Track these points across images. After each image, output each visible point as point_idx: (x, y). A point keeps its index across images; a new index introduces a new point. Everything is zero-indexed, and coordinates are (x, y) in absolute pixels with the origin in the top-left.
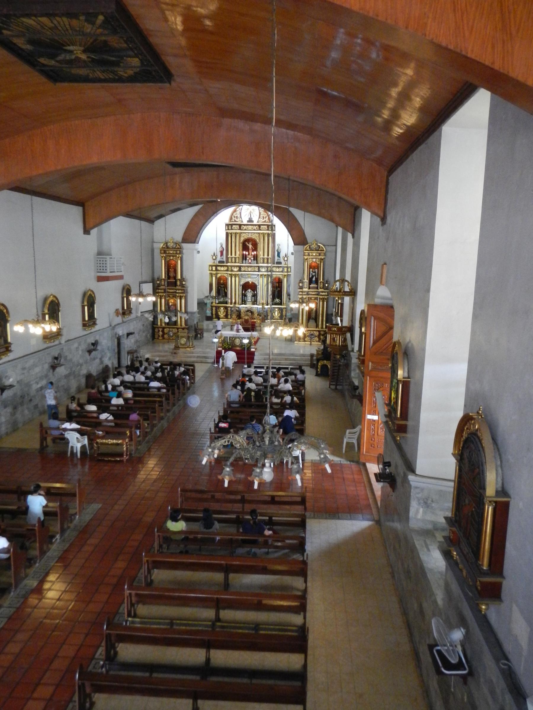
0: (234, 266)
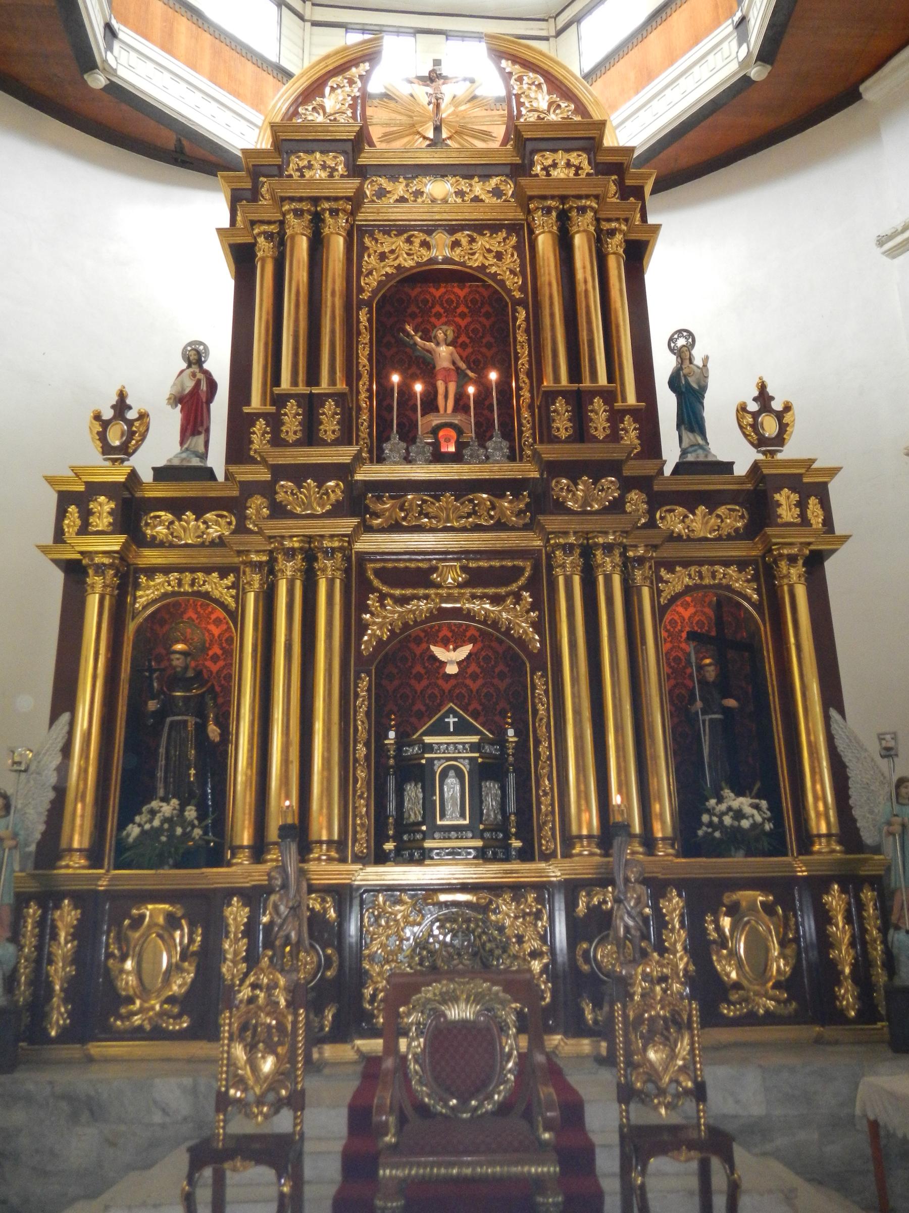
0: (298, 474)
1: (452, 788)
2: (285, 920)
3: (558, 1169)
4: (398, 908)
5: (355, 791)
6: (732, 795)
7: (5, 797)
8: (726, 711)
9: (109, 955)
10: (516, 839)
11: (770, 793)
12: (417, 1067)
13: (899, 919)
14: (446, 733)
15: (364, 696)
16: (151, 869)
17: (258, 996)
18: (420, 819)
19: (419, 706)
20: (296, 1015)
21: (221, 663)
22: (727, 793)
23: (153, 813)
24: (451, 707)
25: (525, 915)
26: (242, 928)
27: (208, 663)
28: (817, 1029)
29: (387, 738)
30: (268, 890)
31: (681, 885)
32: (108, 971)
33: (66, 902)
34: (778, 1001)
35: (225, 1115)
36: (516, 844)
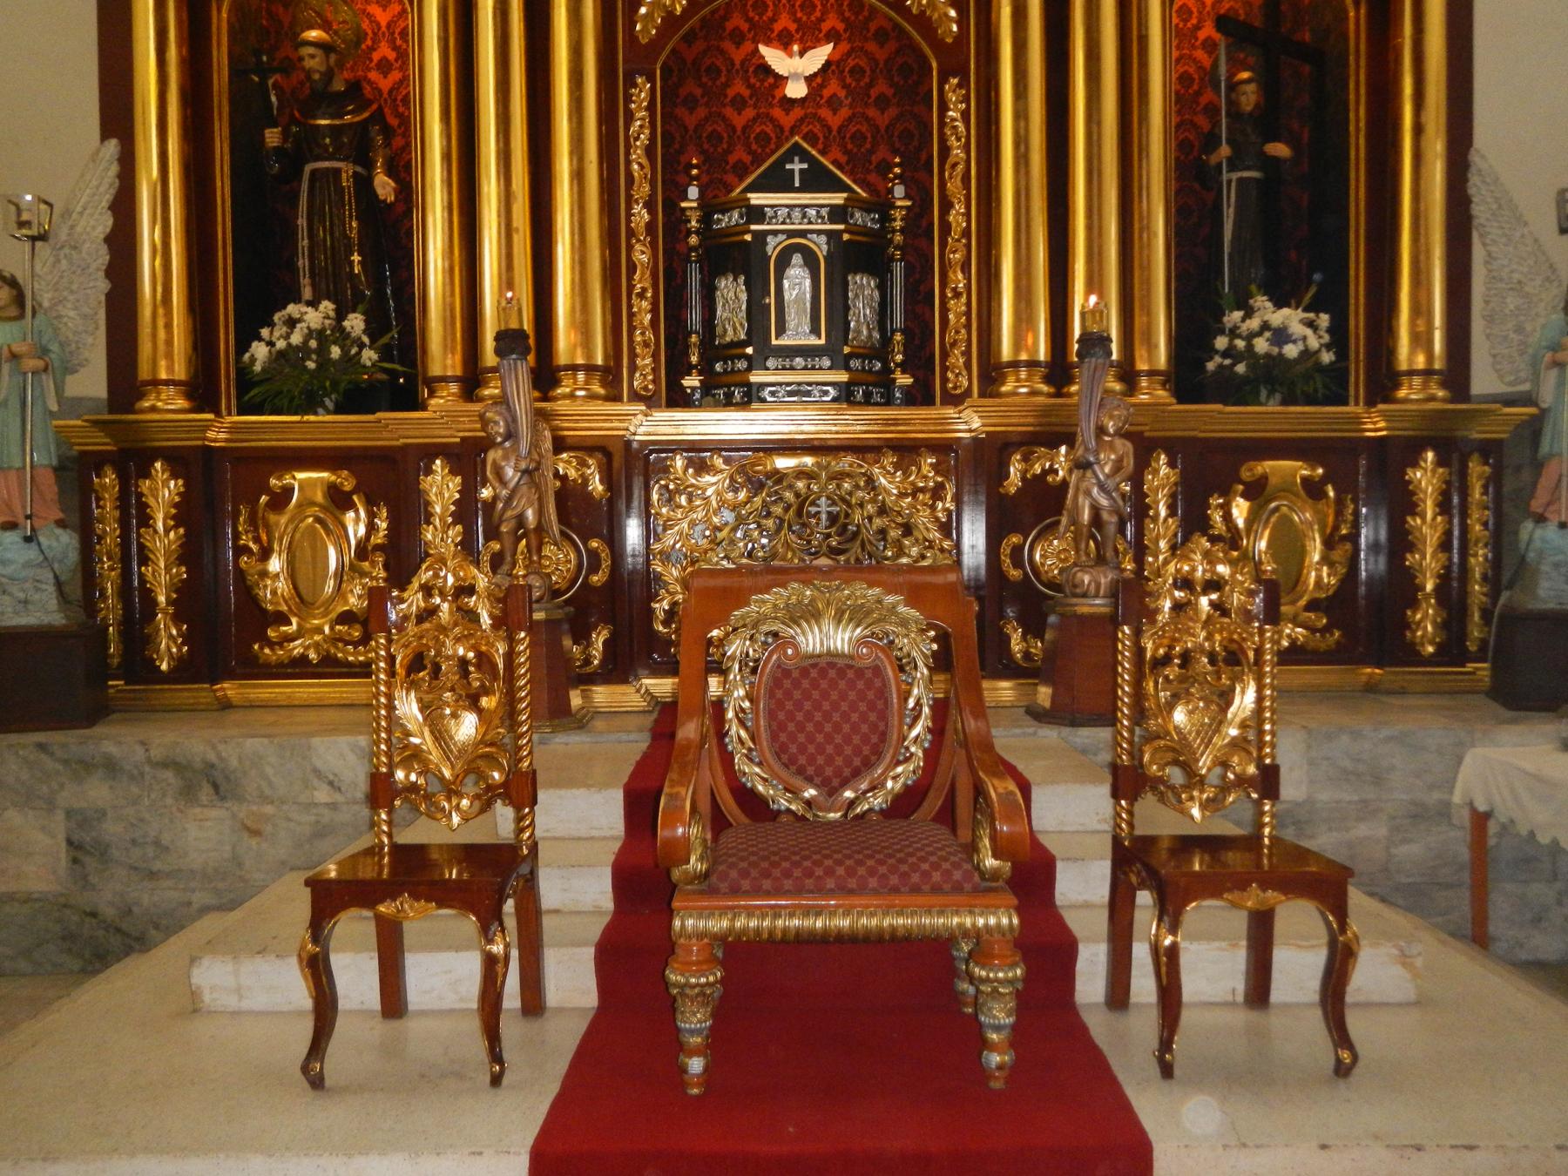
1: (797, 283)
2: (514, 491)
3: (1015, 921)
4: (708, 479)
5: (631, 287)
6: (1269, 305)
7: (13, 283)
8: (1271, 165)
9: (241, 550)
10: (903, 372)
11: (1331, 300)
12: (743, 733)
13: (1549, 504)
14: (789, 188)
15: (642, 119)
16: (296, 414)
17: (436, 609)
18: (743, 337)
19: (740, 154)
20: (511, 641)
21: (395, 75)
22: (1261, 302)
23: (292, 323)
24: (796, 143)
25: (917, 491)
26: (453, 508)
27: (373, 75)
28: (1369, 670)
29: (686, 199)
30: (485, 444)
31: (1173, 448)
32: (240, 574)
33: (158, 465)
34: (1312, 629)
35: (389, 814)
36: (904, 380)
